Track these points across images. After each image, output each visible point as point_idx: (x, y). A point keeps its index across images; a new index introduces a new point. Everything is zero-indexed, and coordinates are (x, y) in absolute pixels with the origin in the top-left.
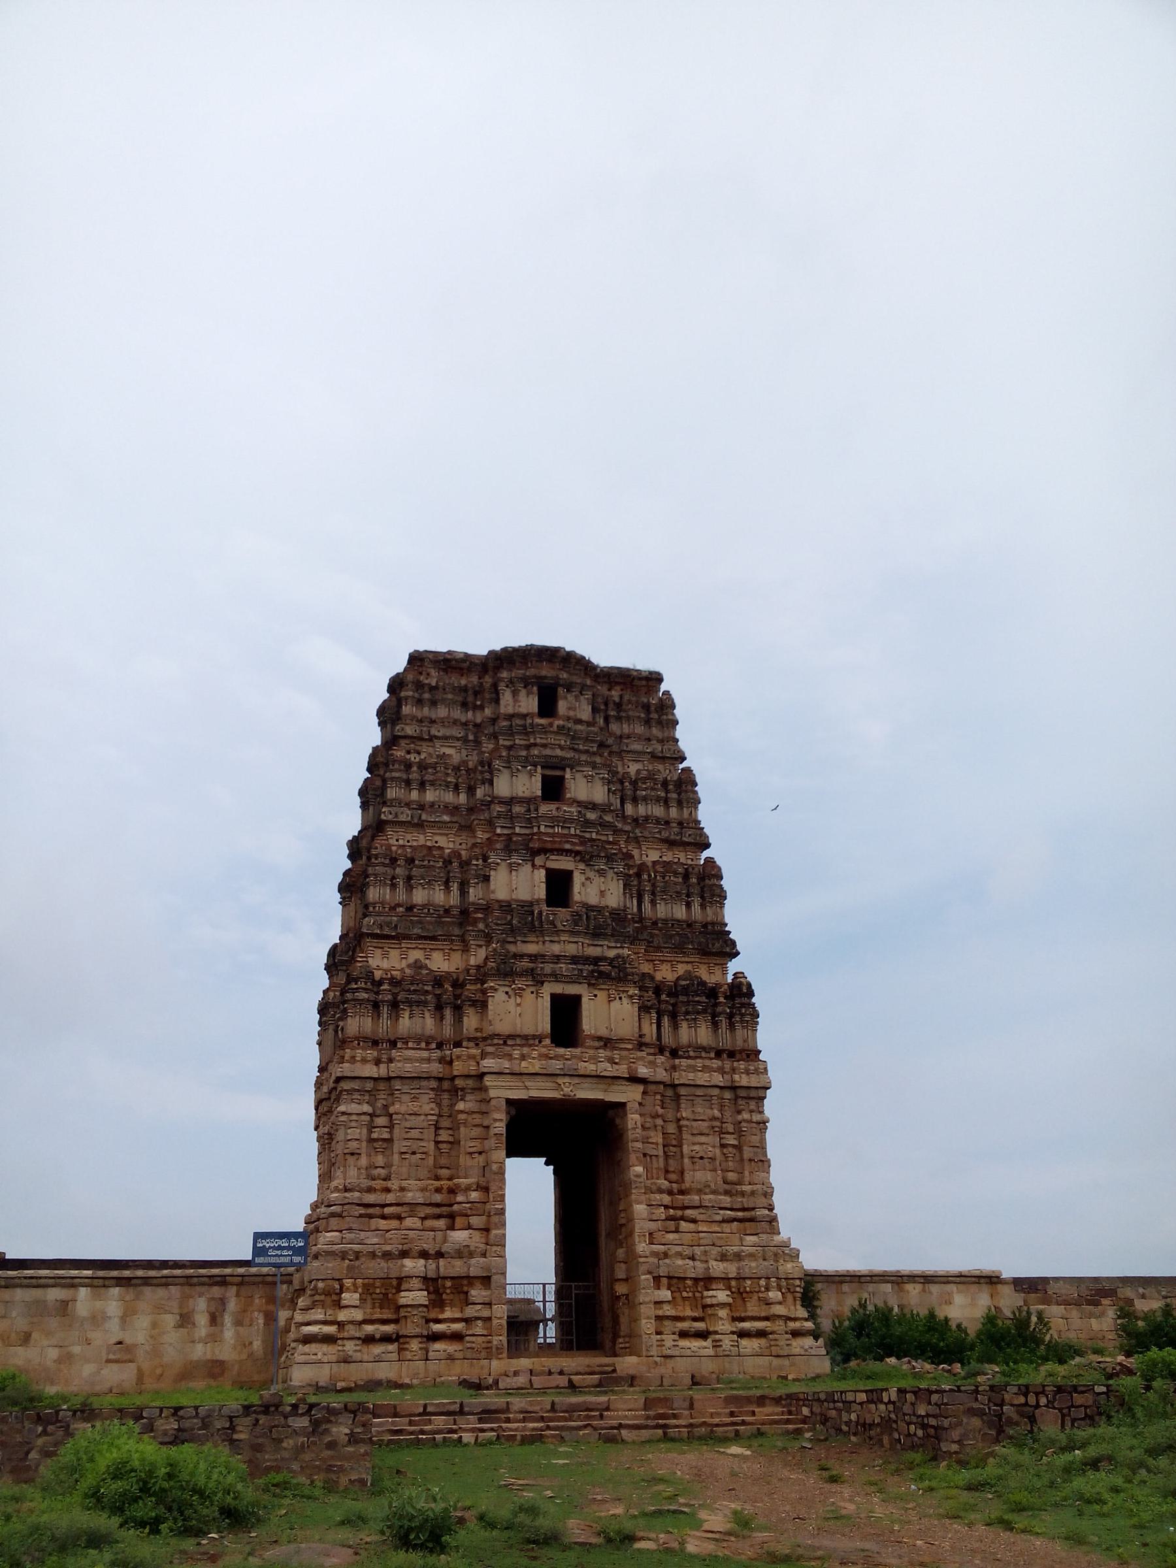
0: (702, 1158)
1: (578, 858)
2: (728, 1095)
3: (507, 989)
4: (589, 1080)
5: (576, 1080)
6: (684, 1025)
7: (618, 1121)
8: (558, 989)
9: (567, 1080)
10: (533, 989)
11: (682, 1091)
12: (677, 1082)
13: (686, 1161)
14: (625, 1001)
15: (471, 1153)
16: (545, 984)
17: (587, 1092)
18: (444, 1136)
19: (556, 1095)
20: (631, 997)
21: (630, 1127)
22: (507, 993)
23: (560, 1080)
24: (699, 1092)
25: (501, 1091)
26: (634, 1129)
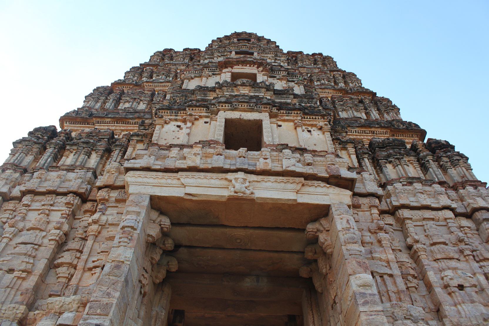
0: (461, 287)
1: (261, 69)
2: (465, 222)
3: (179, 123)
4: (272, 178)
5: (253, 177)
6: (389, 167)
7: (322, 237)
8: (235, 115)
9: (241, 175)
10: (208, 120)
11: (405, 213)
12: (395, 203)
13: (438, 290)
14: (316, 133)
15: (90, 269)
16: (221, 113)
17: (269, 190)
18: (66, 257)
19: (226, 193)
20: (321, 129)
21: (339, 227)
22: (179, 126)
23: (230, 176)
24: (428, 214)
25: (143, 186)
26: (348, 229)
